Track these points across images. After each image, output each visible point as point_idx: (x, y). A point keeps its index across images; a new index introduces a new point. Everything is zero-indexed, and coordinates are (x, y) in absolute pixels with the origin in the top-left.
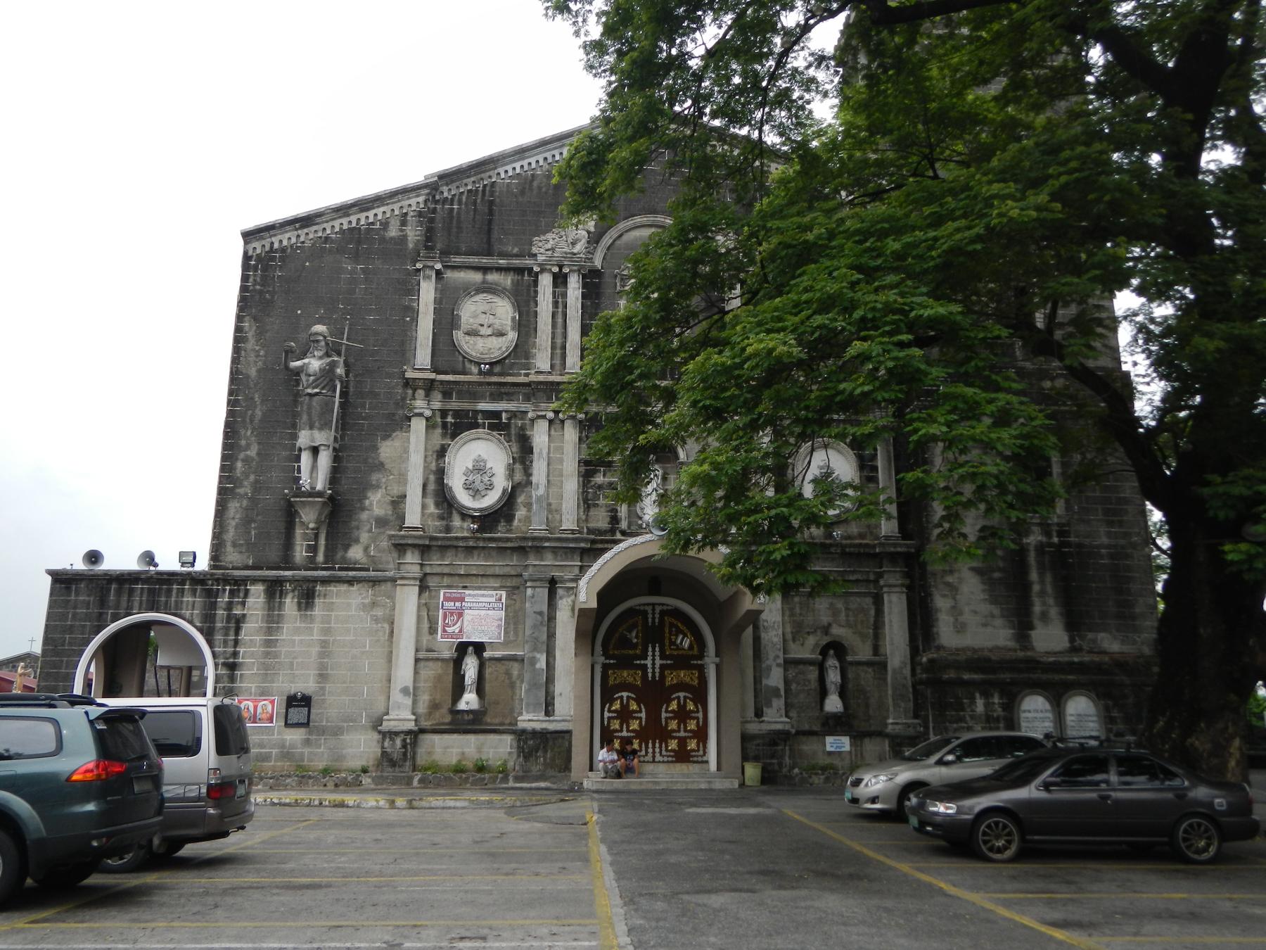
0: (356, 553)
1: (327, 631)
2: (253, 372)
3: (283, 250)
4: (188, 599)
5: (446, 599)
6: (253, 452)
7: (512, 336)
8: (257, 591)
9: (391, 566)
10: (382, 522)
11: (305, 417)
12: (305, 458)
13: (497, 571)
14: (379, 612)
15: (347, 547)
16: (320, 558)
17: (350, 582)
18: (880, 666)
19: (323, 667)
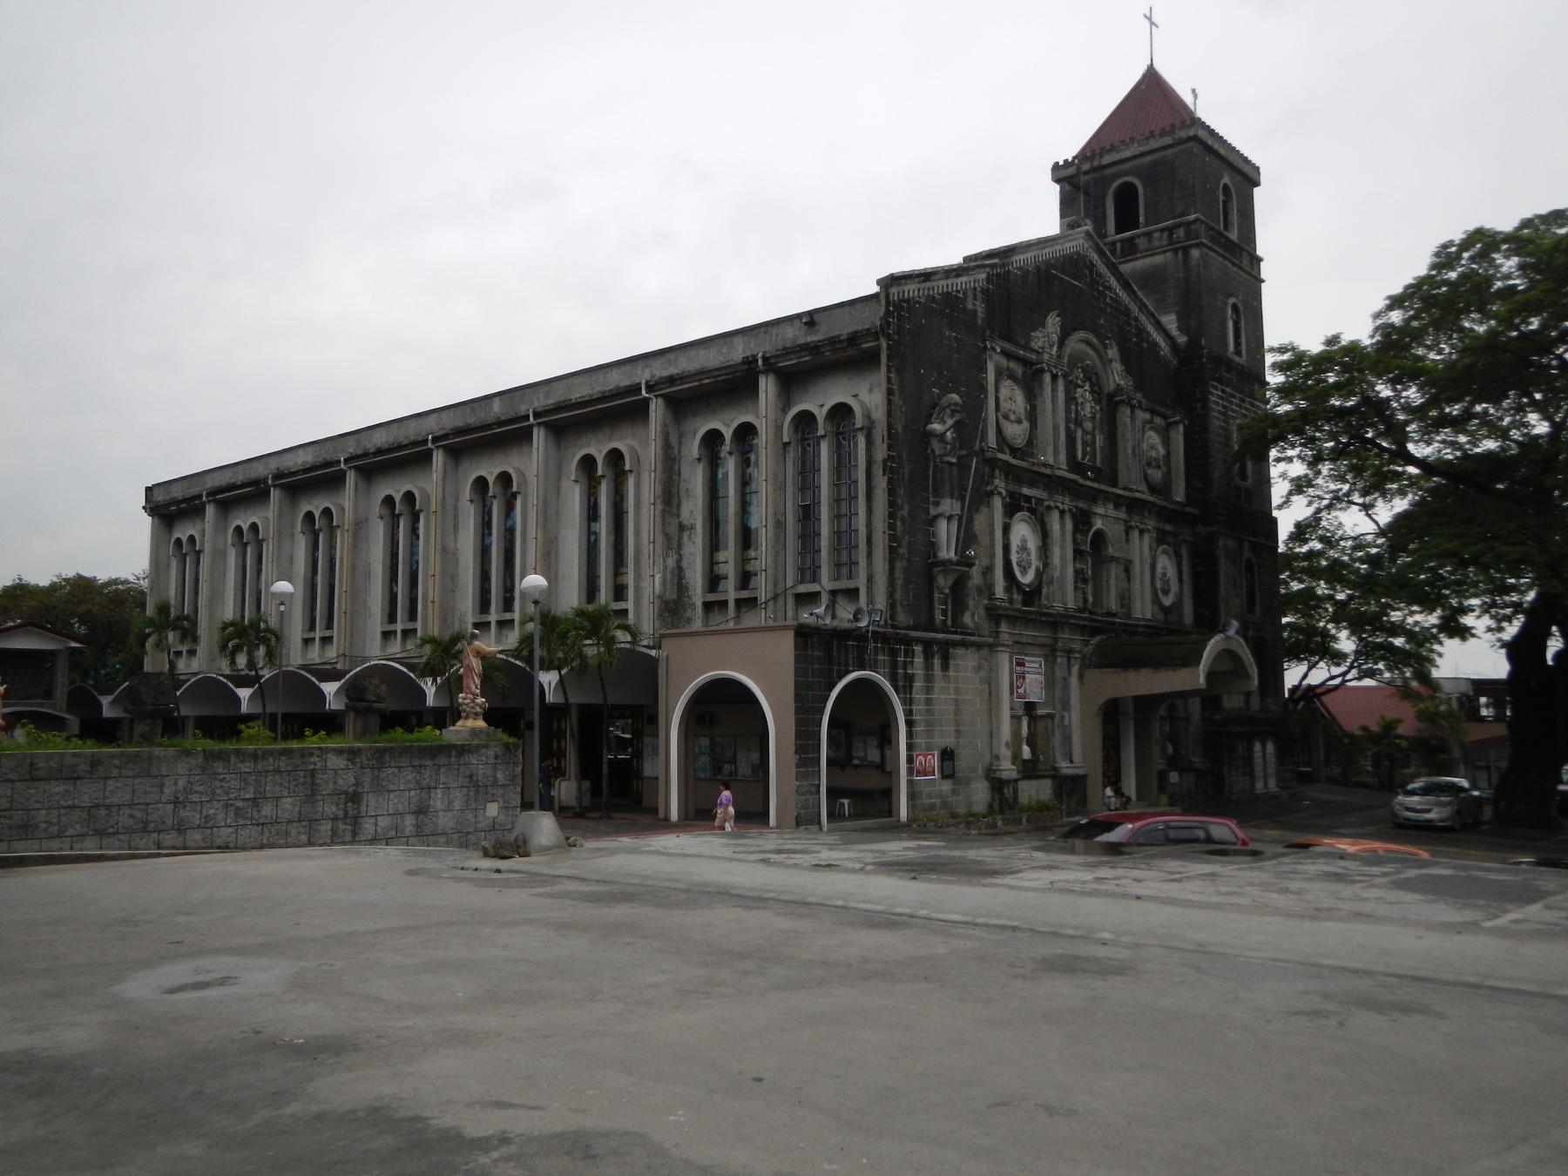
0: (967, 619)
1: (957, 690)
2: (899, 428)
3: (908, 301)
4: (880, 657)
5: (1018, 664)
6: (905, 512)
7: (1026, 424)
8: (918, 649)
9: (986, 632)
10: (979, 590)
11: (948, 487)
12: (943, 525)
13: (1040, 641)
14: (983, 674)
15: (963, 612)
16: (949, 622)
17: (965, 645)
18: (1187, 720)
19: (957, 724)
